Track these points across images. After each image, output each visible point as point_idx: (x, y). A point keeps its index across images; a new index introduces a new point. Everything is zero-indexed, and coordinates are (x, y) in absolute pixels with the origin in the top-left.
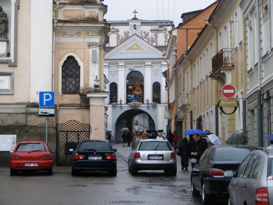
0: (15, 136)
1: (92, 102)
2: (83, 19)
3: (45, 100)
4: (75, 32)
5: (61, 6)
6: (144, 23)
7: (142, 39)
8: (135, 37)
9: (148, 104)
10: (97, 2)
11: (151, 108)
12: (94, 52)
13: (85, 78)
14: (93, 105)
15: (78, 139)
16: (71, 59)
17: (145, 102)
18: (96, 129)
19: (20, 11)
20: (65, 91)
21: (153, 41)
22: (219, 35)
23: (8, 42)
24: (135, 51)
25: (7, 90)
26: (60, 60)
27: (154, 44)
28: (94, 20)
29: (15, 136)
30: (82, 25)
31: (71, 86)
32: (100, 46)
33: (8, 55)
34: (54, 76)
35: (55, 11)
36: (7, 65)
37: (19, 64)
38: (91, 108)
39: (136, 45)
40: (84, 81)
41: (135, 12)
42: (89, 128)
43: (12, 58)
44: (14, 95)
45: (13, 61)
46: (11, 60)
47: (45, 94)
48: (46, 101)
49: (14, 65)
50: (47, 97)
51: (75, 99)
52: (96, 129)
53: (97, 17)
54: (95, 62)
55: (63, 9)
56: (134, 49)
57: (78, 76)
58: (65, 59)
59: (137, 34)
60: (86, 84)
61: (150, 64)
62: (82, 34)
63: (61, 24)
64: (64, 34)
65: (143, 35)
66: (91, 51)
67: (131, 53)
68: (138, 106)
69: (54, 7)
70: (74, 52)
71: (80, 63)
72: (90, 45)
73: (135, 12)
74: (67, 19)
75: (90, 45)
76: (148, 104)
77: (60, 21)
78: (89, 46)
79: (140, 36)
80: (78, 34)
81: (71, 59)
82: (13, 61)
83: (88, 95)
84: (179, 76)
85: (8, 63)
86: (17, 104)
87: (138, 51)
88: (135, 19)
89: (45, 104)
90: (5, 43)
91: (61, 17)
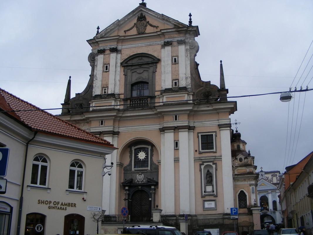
0: (219, 229)
1: (253, 212)
2: (246, 173)
3: (233, 212)
4: (243, 179)
5: (236, 168)
6: (266, 173)
7: (266, 180)
8: (262, 180)
9: (271, 211)
10: (252, 165)
11: (273, 214)
12: (253, 188)
13: (249, 201)
14: (254, 213)
15: (248, 229)
16: (242, 192)
17: (270, 210)
18: (256, 225)
19: (217, 172)
20: (240, 207)
21: (271, 181)
22: (309, 176)
23: (213, 186)
24: (263, 186)
25: (214, 208)
26: (237, 192)
27: (272, 182)
28: (251, 173)
29: (219, 229)
30: (246, 176)
31: (243, 204)
32: (255, 185)
33: (213, 191)
34: (235, 200)
35: (233, 170)
36: (213, 196)
37: (218, 196)
38: (253, 215)
39: (263, 183)
40: (249, 202)
41: (261, 168)
42: (253, 224)
43: (215, 193)
44: (217, 210)
45: (215, 194)
46: (215, 194)
47: (233, 209)
48: (234, 212)
49: (216, 196)
50: (234, 210)
51: (245, 210)
52: (256, 225)
53: (253, 172)
54: (253, 193)
55: (237, 169)
56: (262, 185)
57: (246, 200)
58: (239, 192)
59: (263, 178)
60: (250, 203)
61: (271, 192)
62: (246, 180)
63: (236, 176)
64: (238, 180)
65: (266, 178)
66: (251, 187)
67: (261, 187)
68: (266, 213)
69: (232, 169)
70: (243, 189)
71: (247, 194)
72: (250, 185)
73: (261, 168)
74: (239, 173)
75: (250, 185)
76: (271, 211)
77: (236, 175)
78: (250, 185)
79: (265, 179)
80: (245, 180)
81: (242, 192)
82: (215, 194)
83: (252, 209)
84: (287, 197)
85: (213, 195)
86: (218, 214)
87: (264, 186)
88: (262, 171)
89: (233, 214)
90: (211, 186)
91: (236, 173)
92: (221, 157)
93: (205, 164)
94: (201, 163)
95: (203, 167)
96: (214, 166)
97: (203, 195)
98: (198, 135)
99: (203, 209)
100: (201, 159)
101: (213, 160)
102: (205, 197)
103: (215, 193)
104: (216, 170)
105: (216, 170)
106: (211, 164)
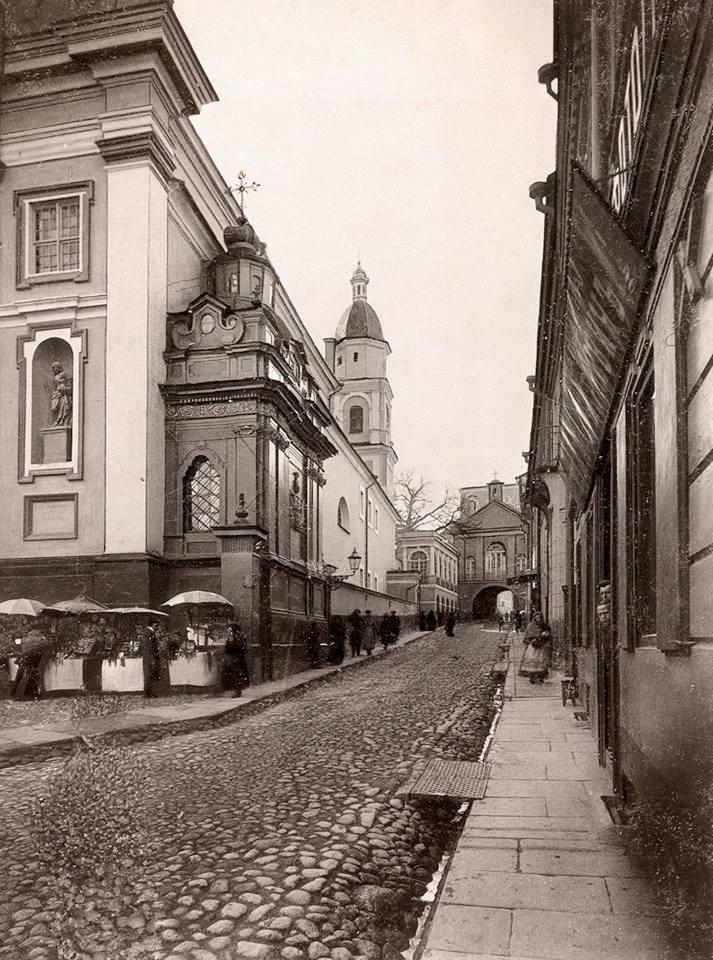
19: (87, 366)
45: (76, 471)
82: (76, 471)
92: (103, 302)
93: (42, 336)
94: (24, 332)
95: (30, 349)
96: (76, 345)
97: (27, 474)
98: (17, 203)
99: (25, 537)
100: (23, 315)
101: (70, 316)
102: (33, 483)
103: (74, 464)
104: (85, 360)
105: (85, 360)
106: (64, 334)
